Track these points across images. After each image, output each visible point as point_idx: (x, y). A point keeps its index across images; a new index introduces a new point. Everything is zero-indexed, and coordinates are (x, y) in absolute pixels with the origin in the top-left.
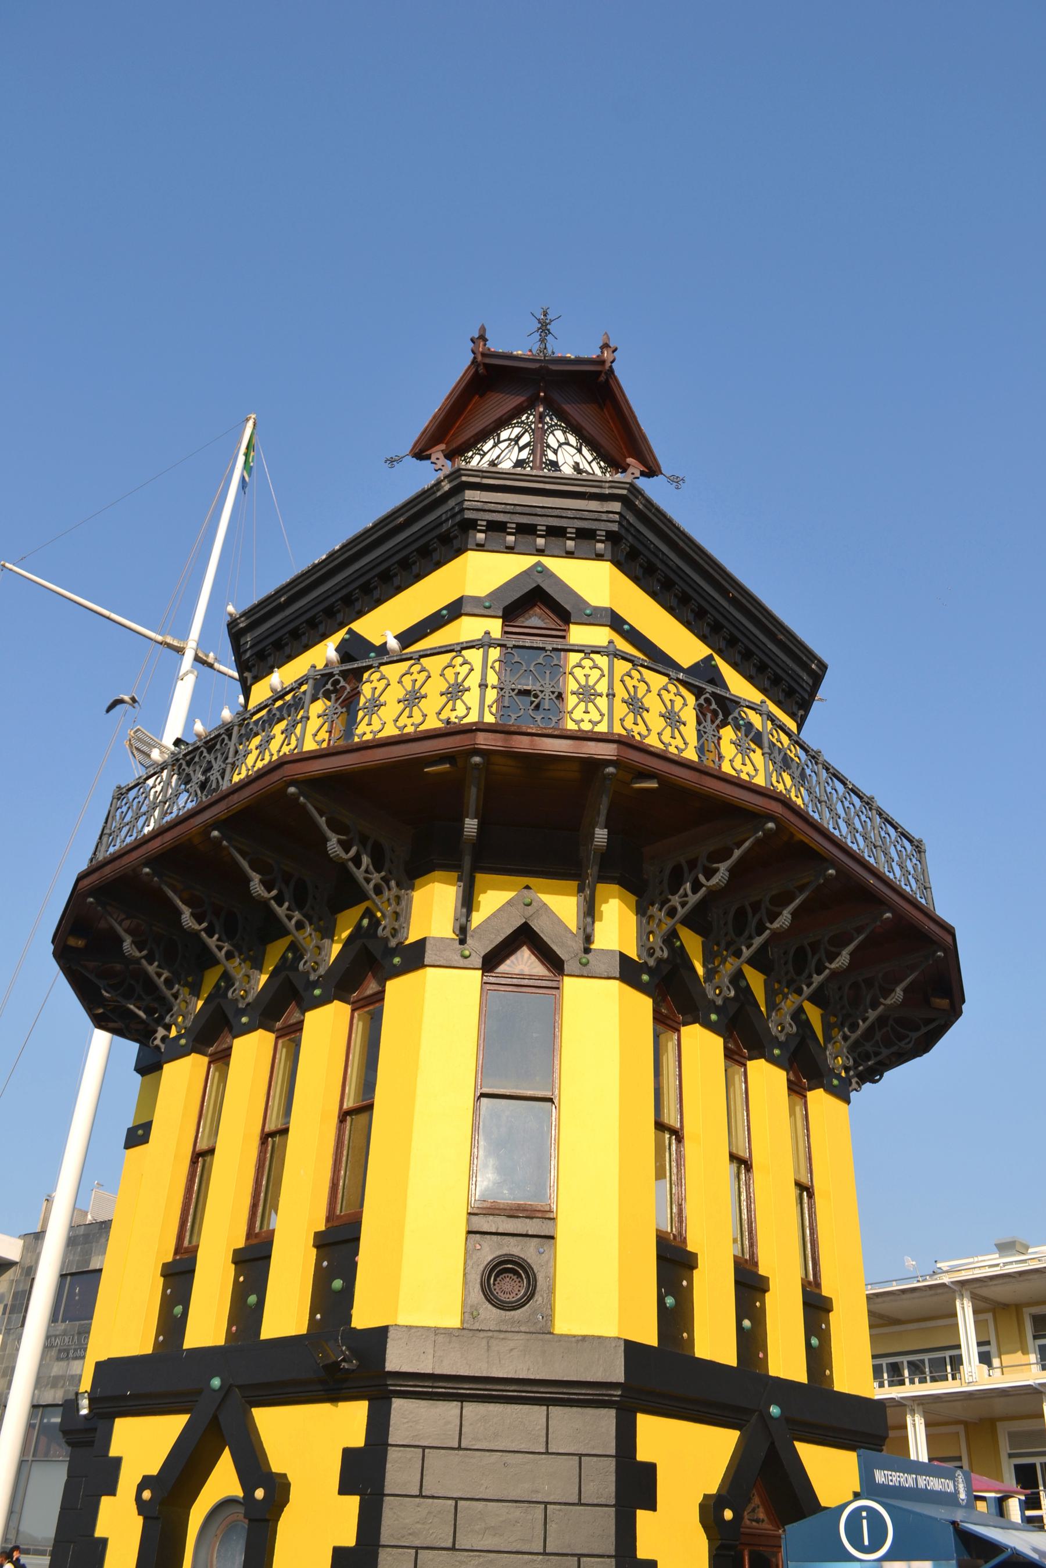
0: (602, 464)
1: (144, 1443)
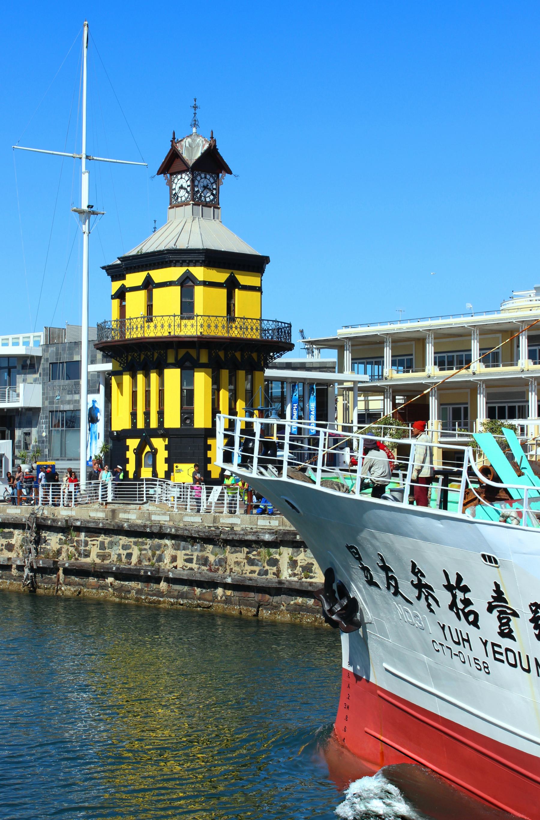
1: (133, 443)
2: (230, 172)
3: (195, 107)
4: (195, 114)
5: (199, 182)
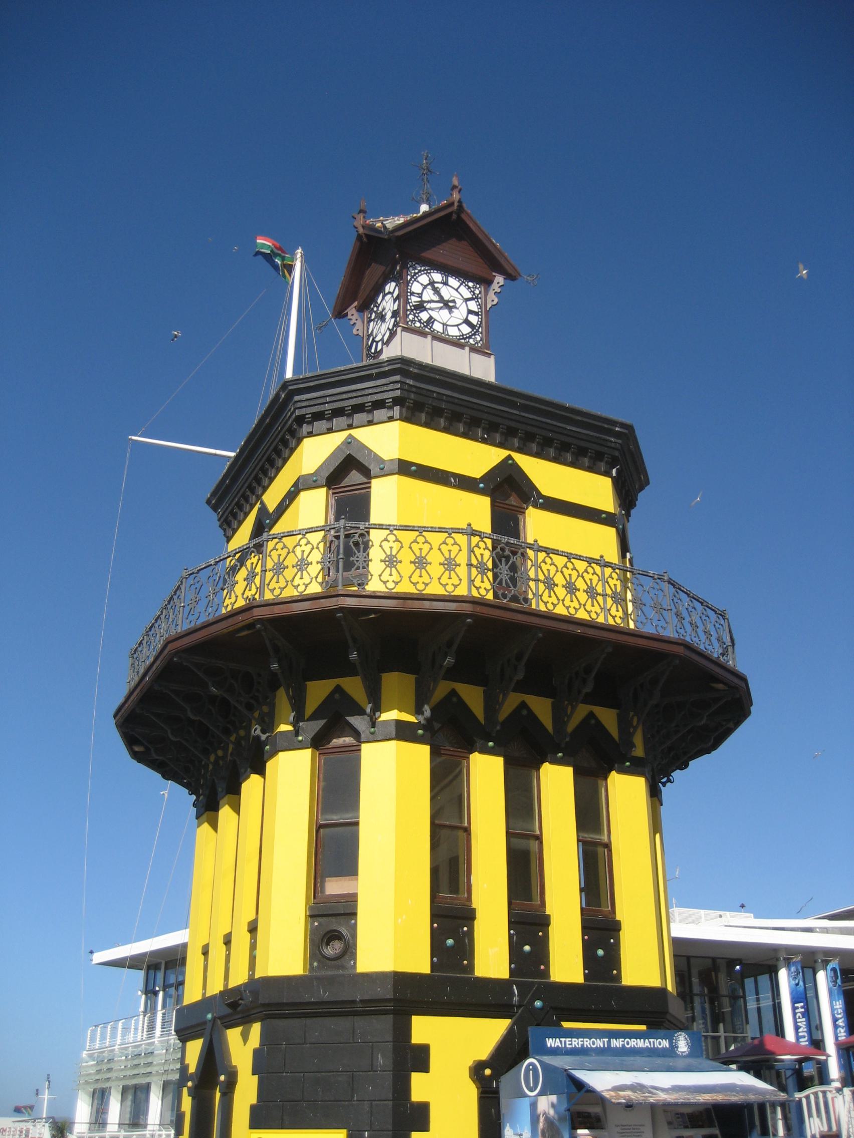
0: (471, 284)
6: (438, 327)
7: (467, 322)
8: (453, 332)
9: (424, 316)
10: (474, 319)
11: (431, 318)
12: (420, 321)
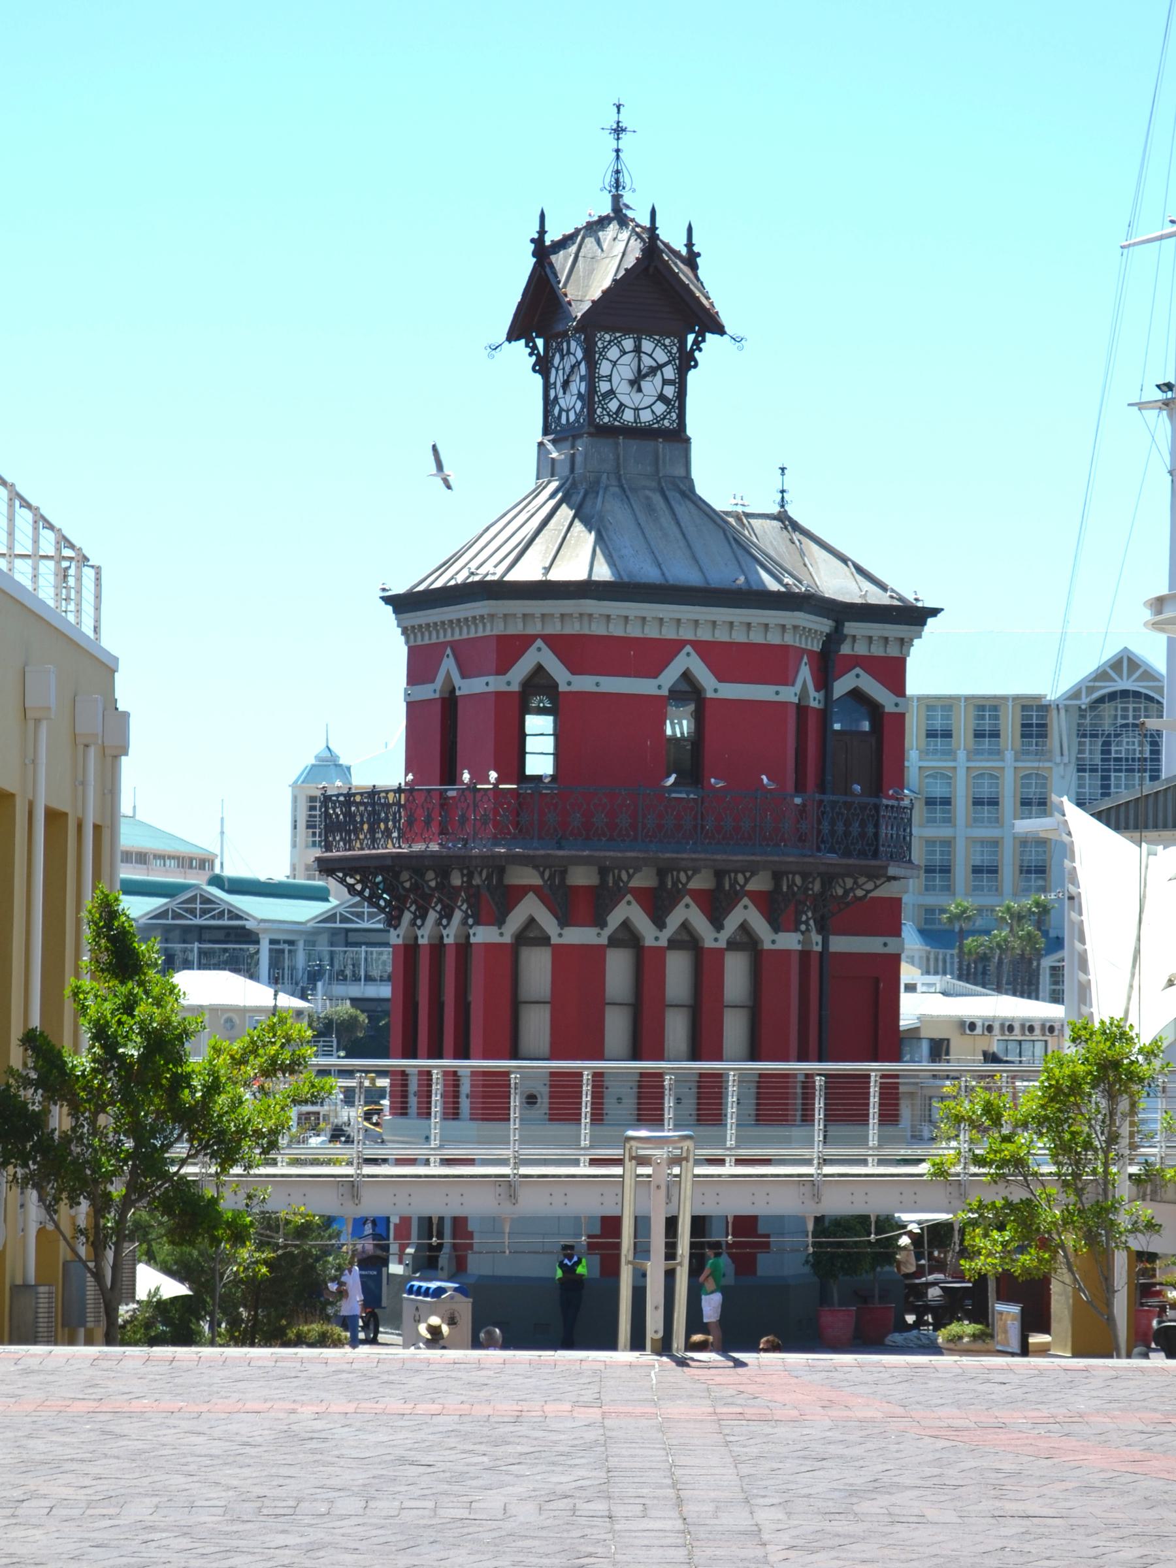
0: (667, 342)
2: (720, 330)
3: (618, 131)
4: (618, 151)
5: (614, 364)
6: (628, 416)
7: (662, 398)
8: (646, 416)
9: (613, 405)
10: (669, 391)
11: (621, 405)
12: (609, 415)
